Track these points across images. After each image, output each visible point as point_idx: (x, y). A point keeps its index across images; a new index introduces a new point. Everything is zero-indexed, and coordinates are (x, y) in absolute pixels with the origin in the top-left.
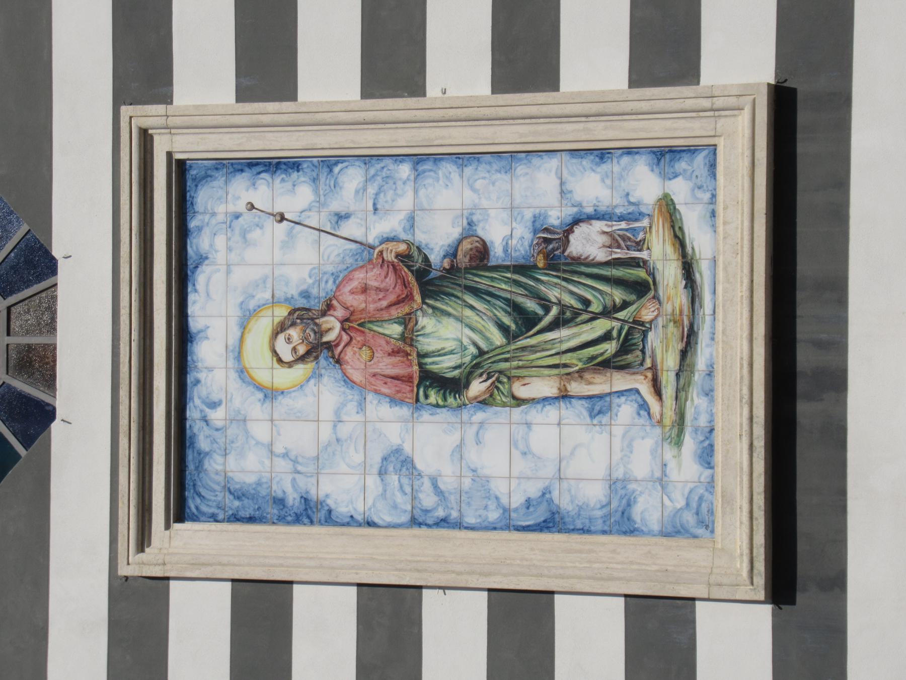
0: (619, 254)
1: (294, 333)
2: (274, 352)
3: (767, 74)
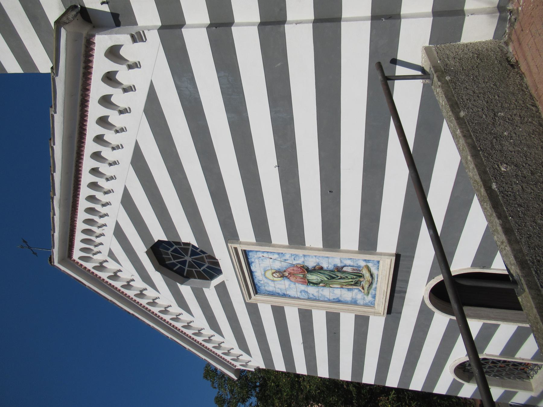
0: (355, 271)
1: (278, 274)
2: (273, 276)
3: (394, 251)
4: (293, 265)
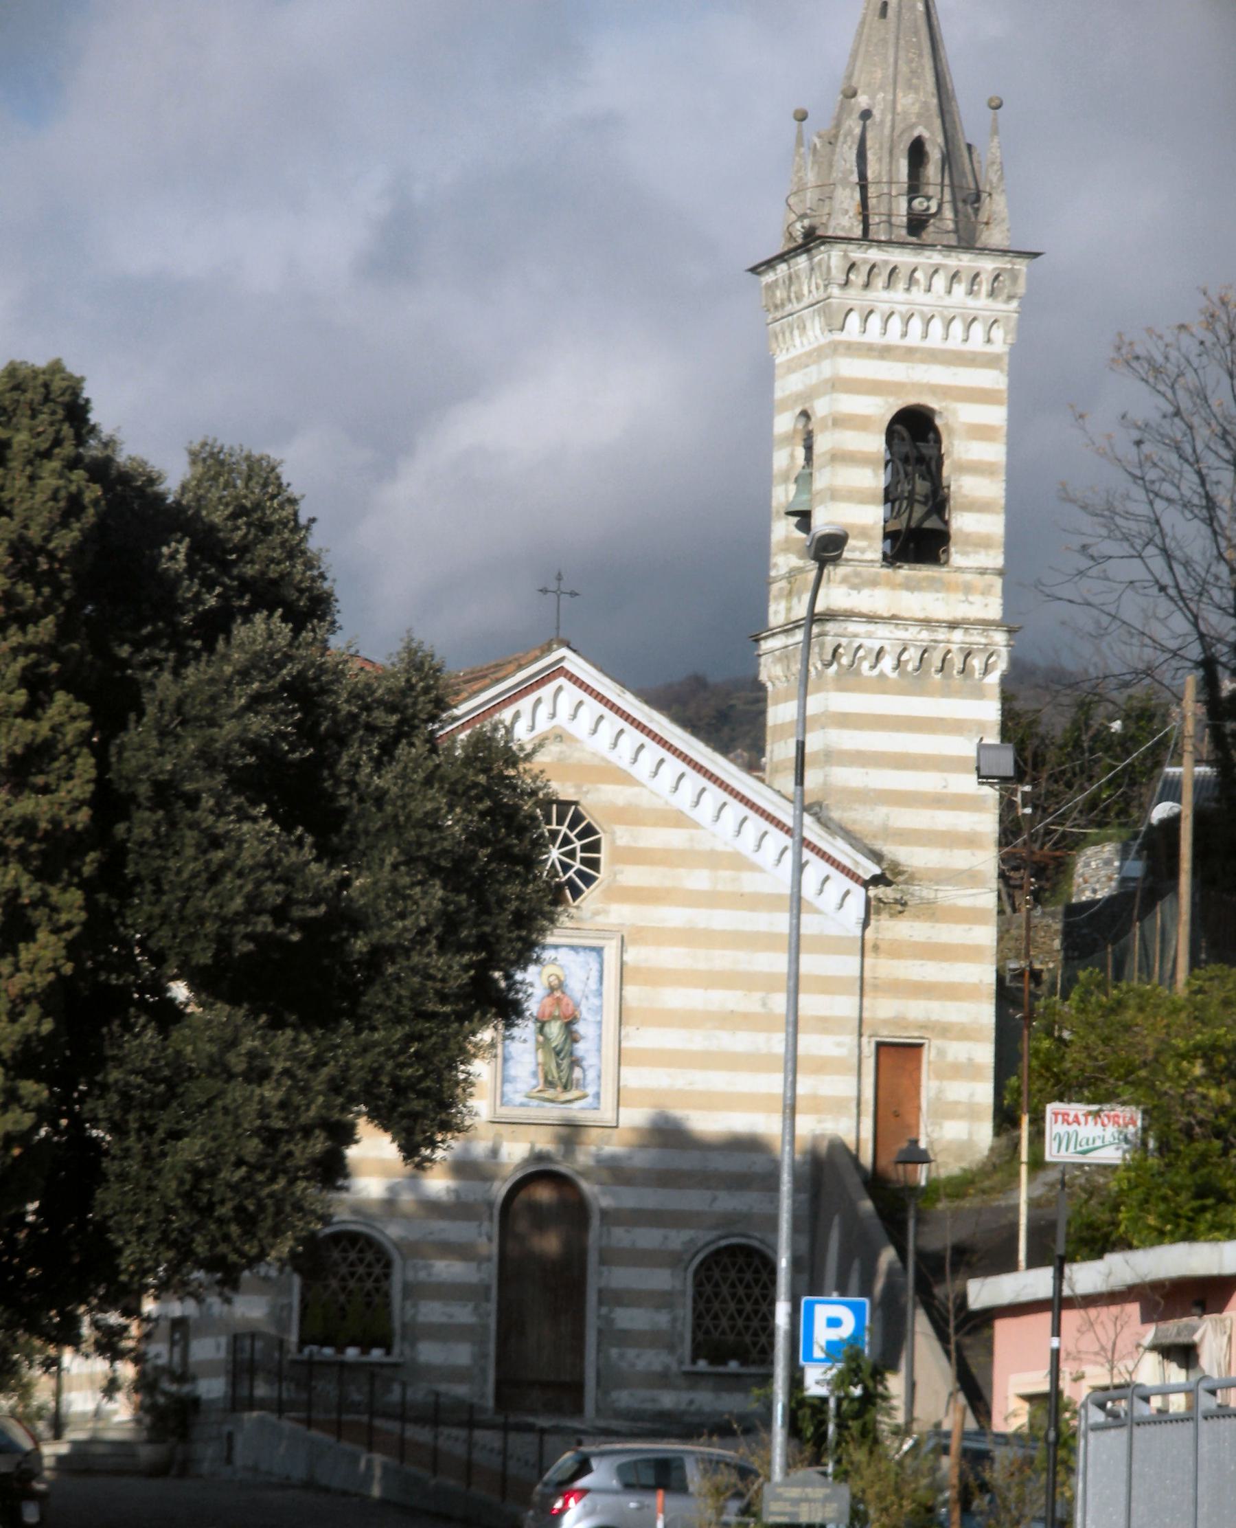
4: (577, 1006)
